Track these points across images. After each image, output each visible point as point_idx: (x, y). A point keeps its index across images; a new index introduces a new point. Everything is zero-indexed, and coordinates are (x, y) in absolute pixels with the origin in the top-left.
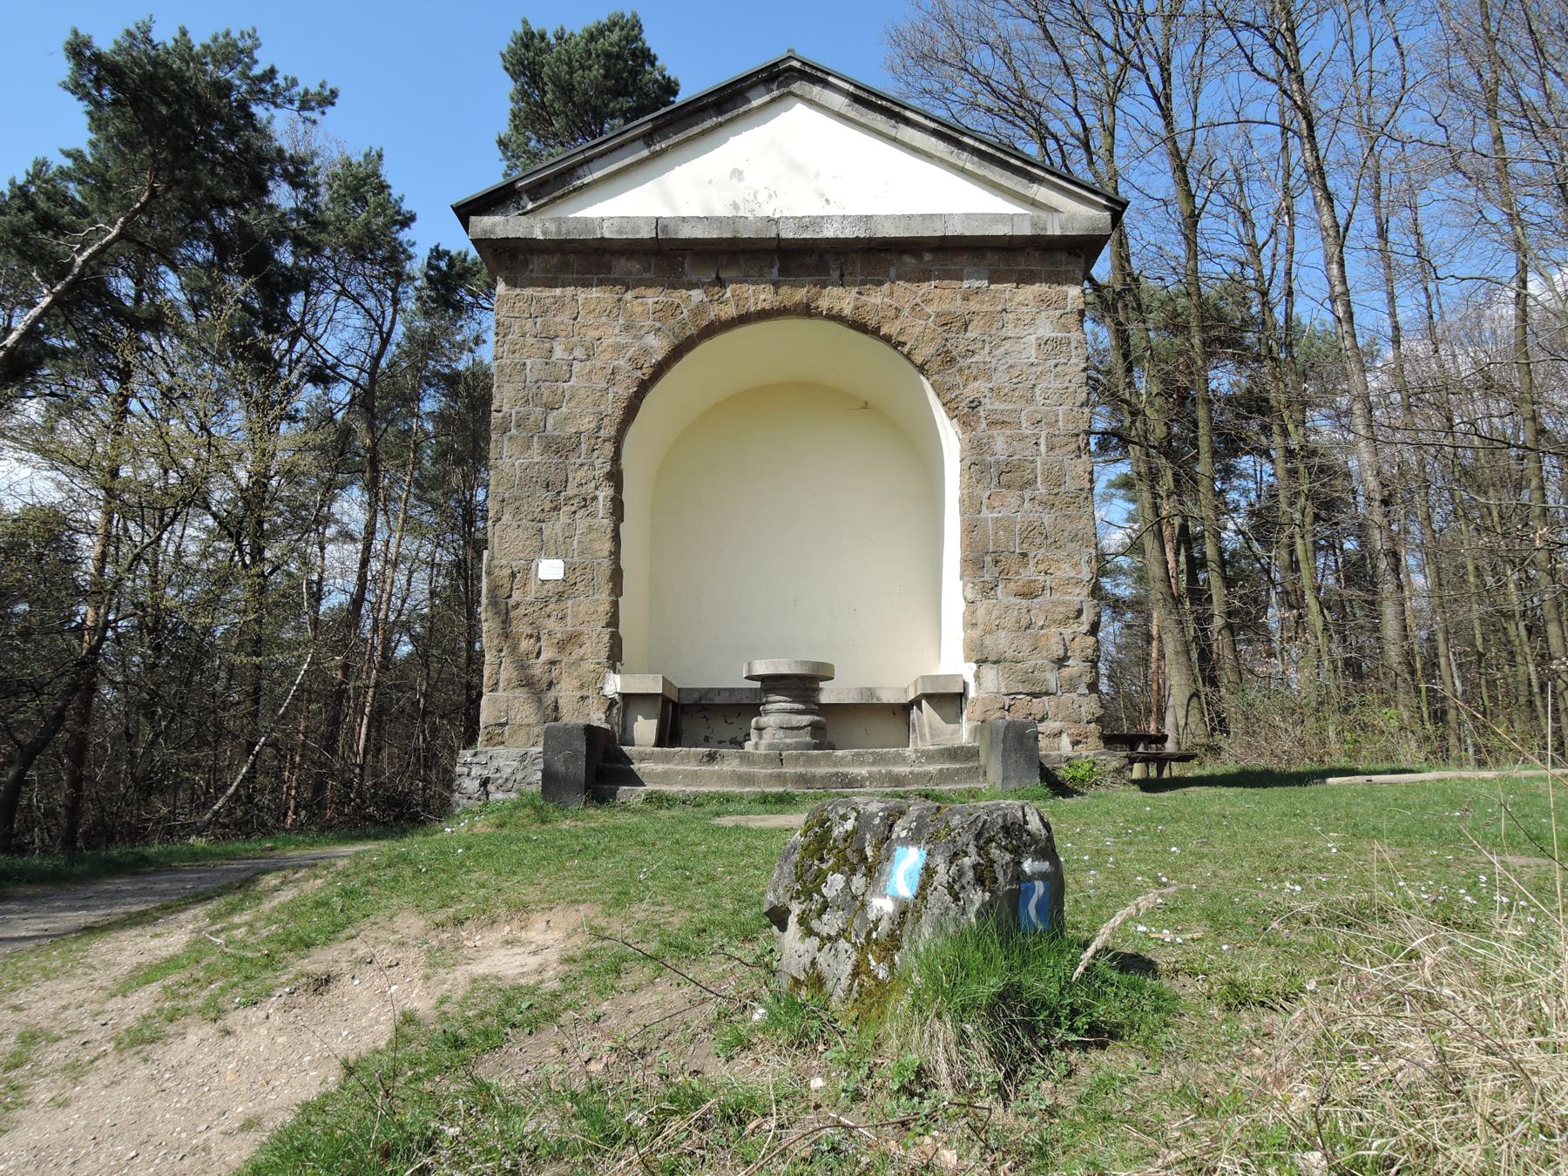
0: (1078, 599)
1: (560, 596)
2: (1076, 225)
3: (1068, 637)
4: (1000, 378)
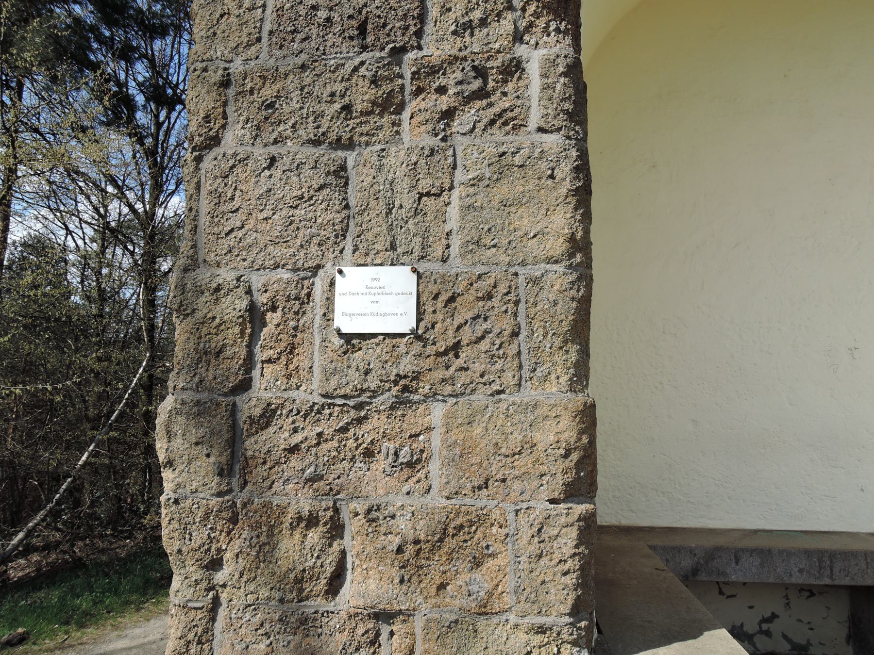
1: (406, 391)
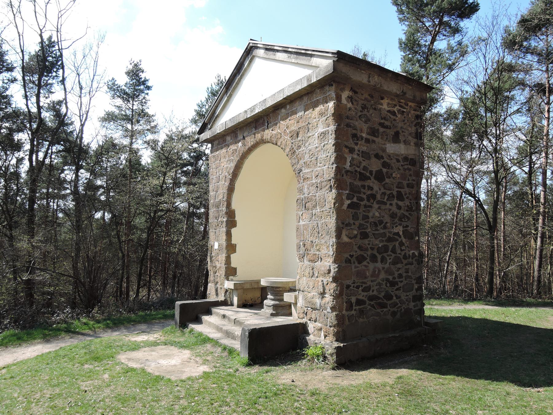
0: (328, 264)
2: (321, 73)
3: (325, 283)
4: (307, 158)
